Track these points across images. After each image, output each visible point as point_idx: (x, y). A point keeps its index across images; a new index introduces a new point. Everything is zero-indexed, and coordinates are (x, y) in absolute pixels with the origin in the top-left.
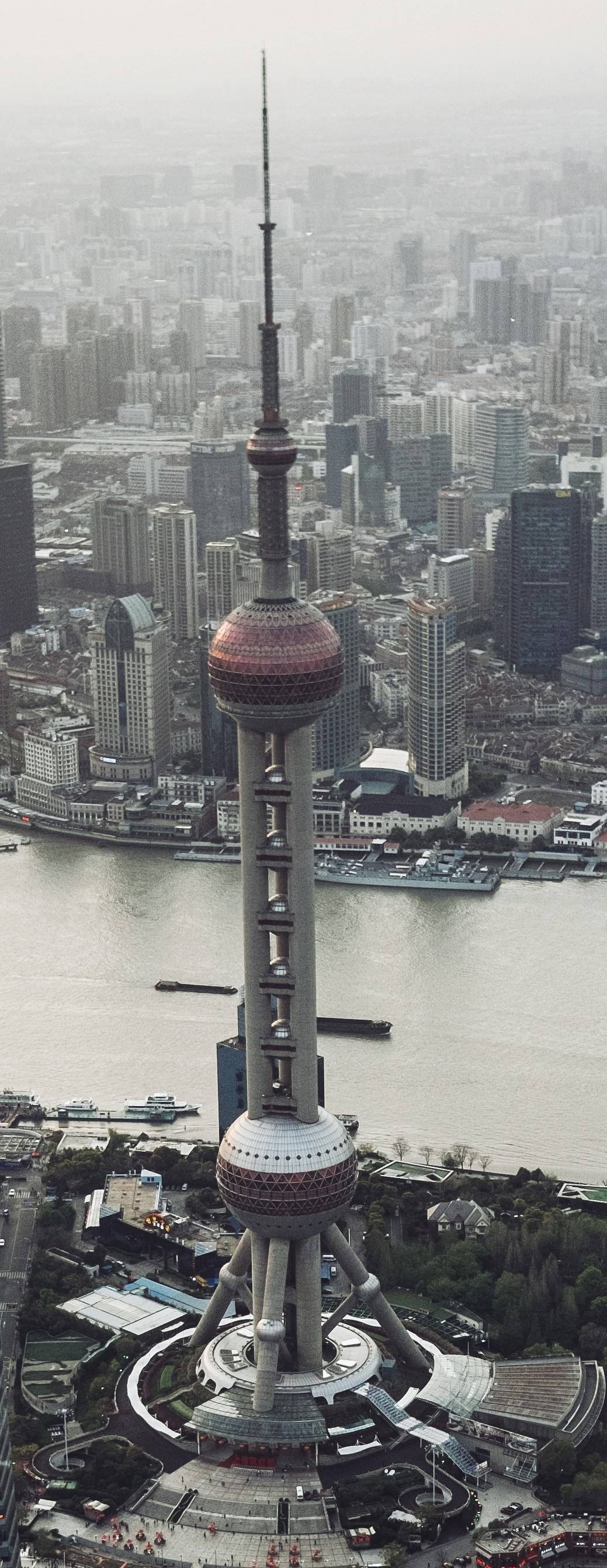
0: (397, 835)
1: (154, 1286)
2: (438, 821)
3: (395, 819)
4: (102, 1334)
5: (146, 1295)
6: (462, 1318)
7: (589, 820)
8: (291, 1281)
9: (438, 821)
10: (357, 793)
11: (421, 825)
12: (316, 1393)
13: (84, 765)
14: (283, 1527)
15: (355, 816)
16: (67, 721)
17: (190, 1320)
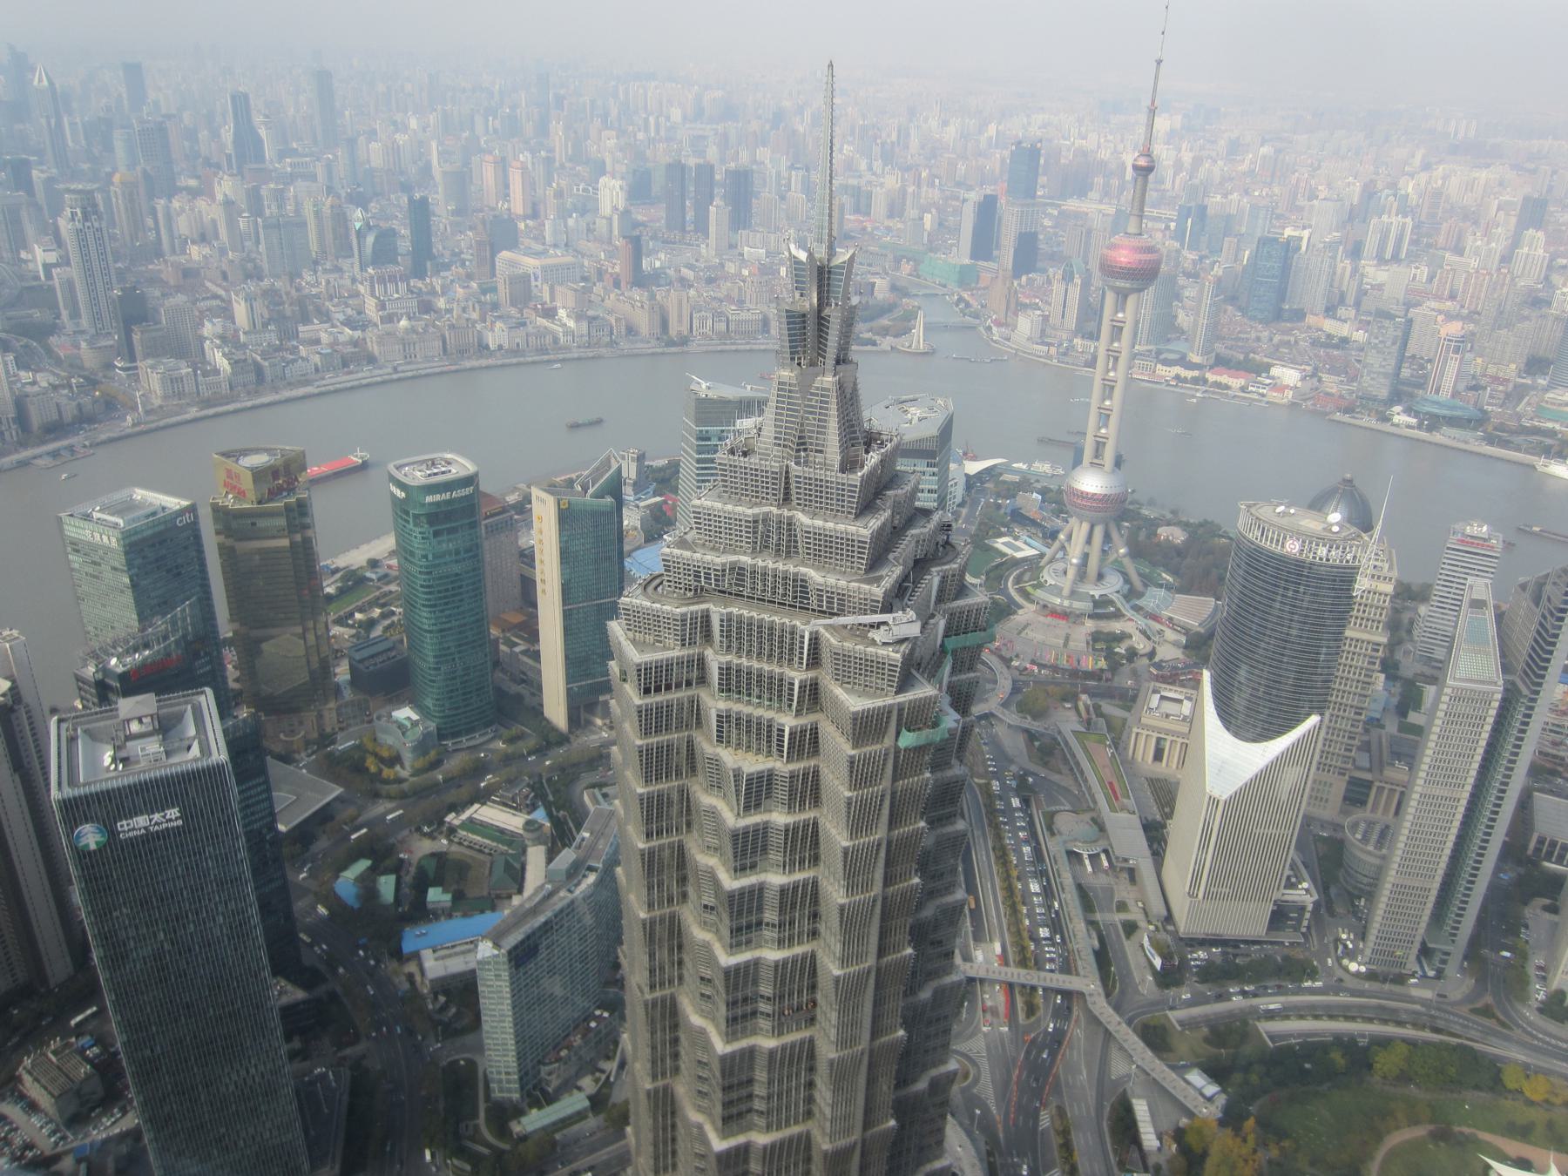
0: (1177, 377)
1: (1029, 540)
2: (1196, 373)
3: (1177, 370)
4: (1005, 555)
5: (1025, 543)
6: (1164, 575)
7: (1268, 381)
8: (1089, 541)
9: (1196, 373)
10: (1162, 357)
11: (1189, 374)
12: (1092, 593)
13: (1043, 331)
14: (1065, 645)
15: (1159, 366)
16: (1038, 312)
17: (1042, 555)
